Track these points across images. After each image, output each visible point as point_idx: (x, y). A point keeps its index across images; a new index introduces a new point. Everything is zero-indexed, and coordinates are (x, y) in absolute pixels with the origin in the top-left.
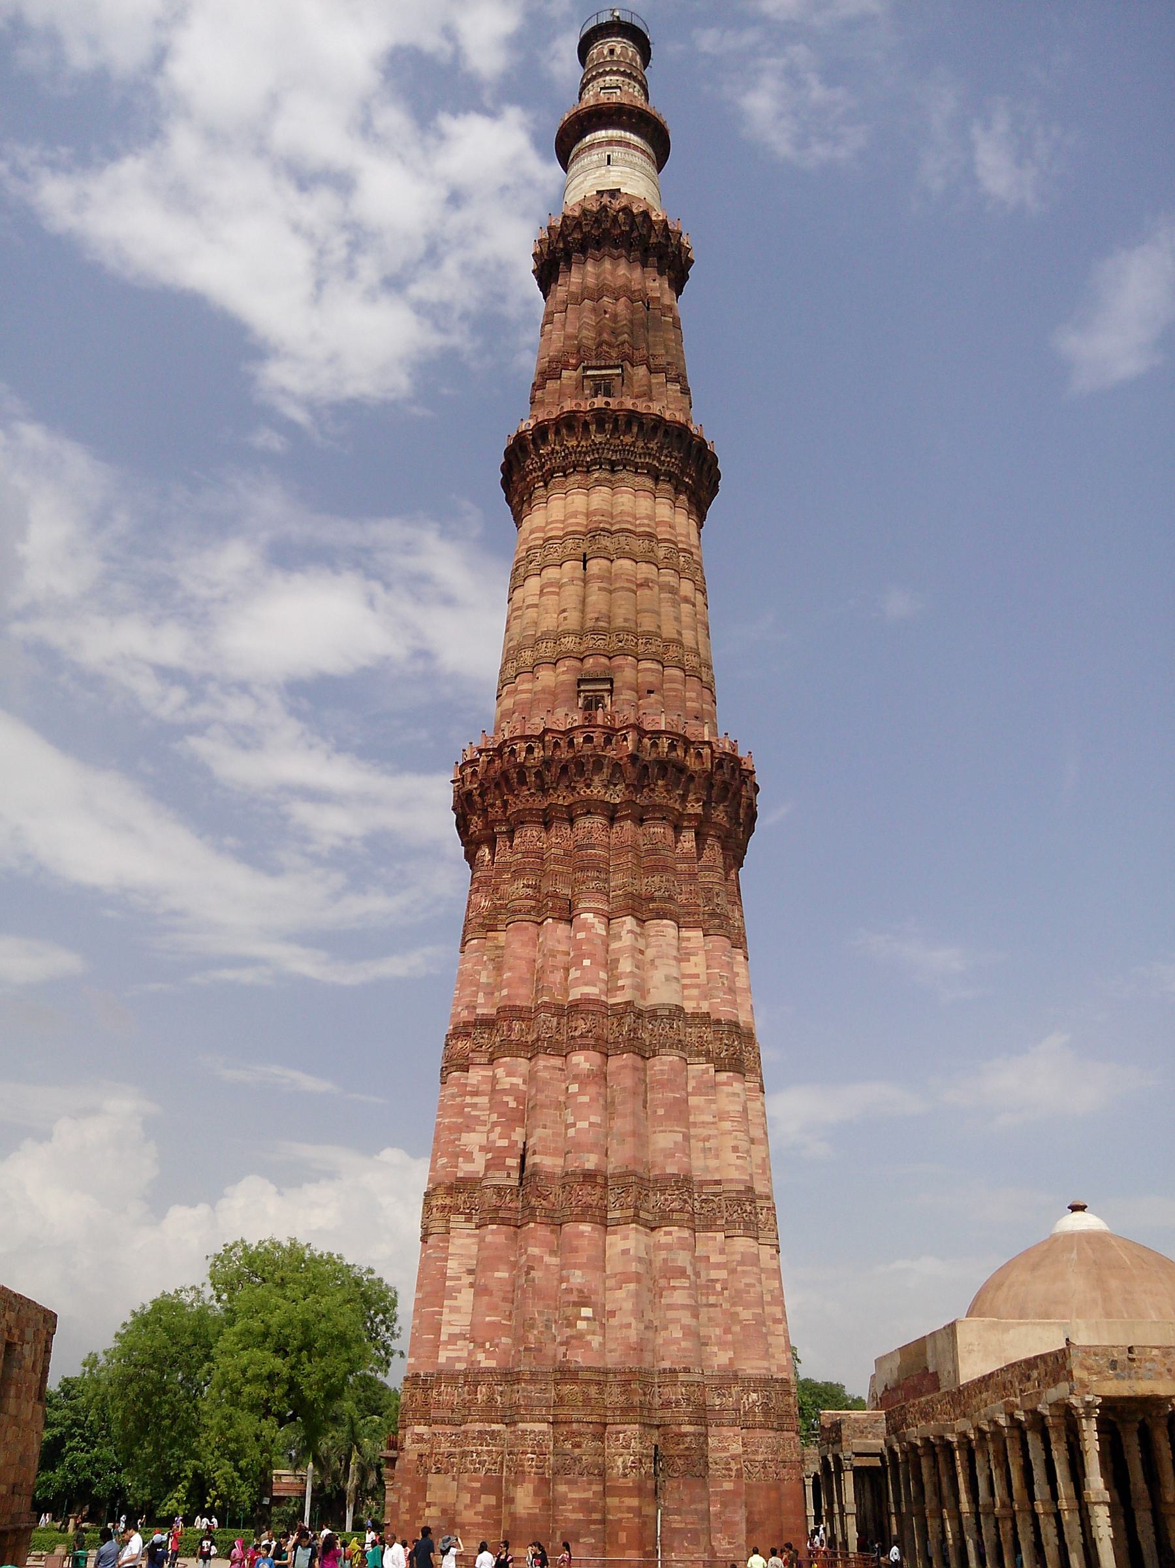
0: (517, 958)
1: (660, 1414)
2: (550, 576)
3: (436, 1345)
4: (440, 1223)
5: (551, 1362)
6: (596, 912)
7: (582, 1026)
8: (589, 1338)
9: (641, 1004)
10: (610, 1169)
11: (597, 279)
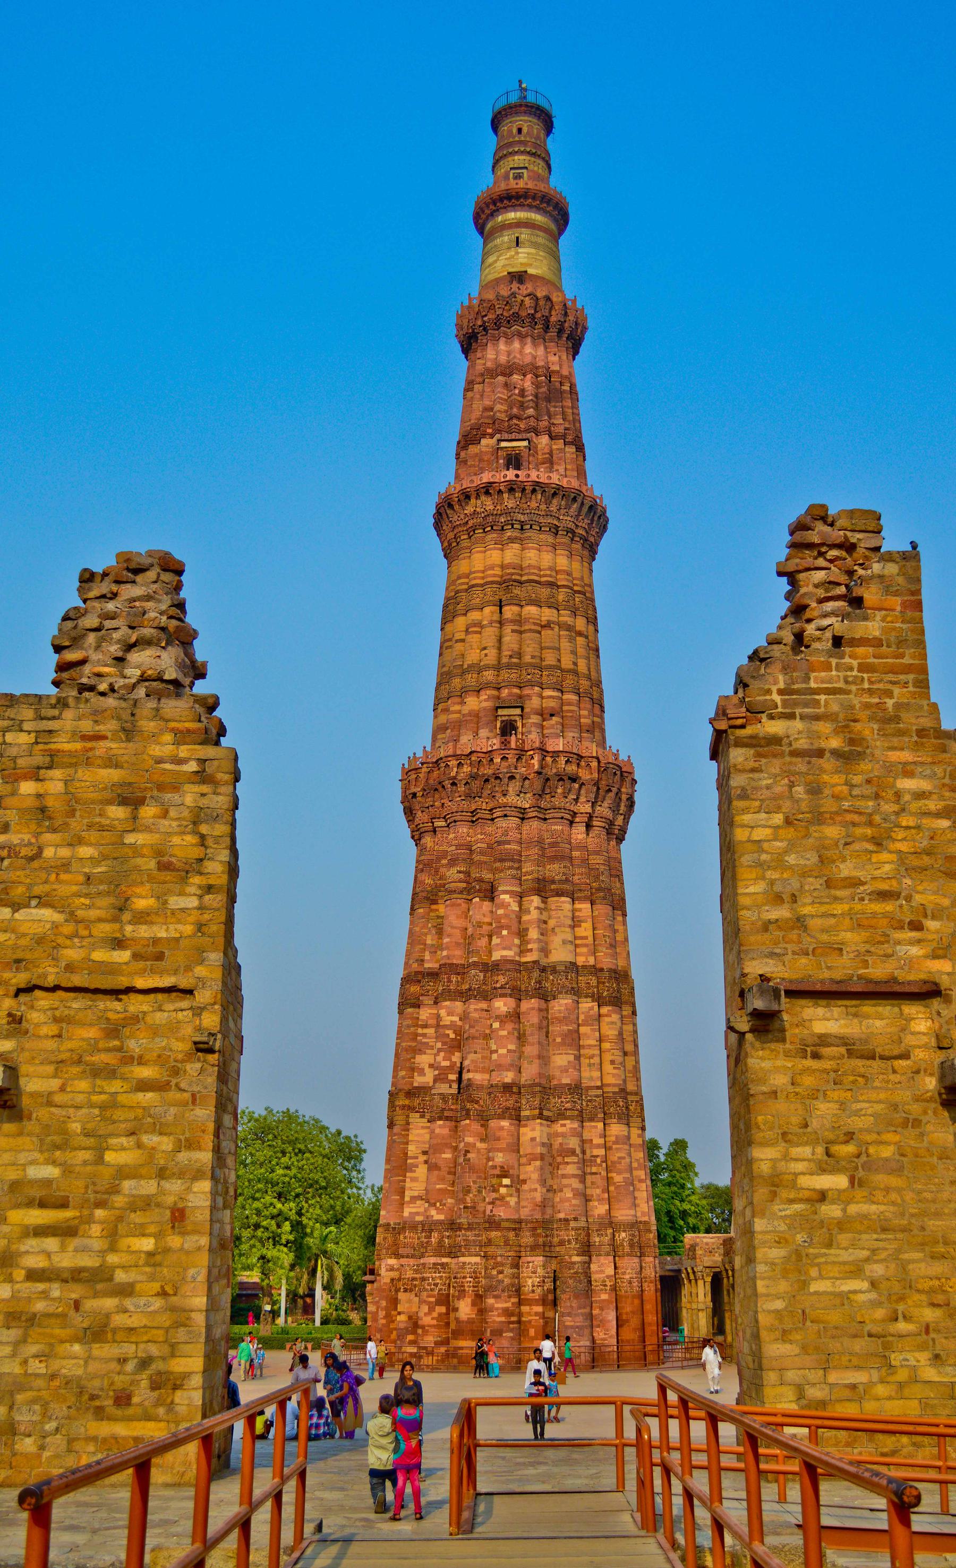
0: (452, 927)
1: (557, 1249)
3: (402, 1204)
7: (502, 980)
8: (508, 1199)
9: (544, 962)
10: (523, 1081)
11: (509, 355)
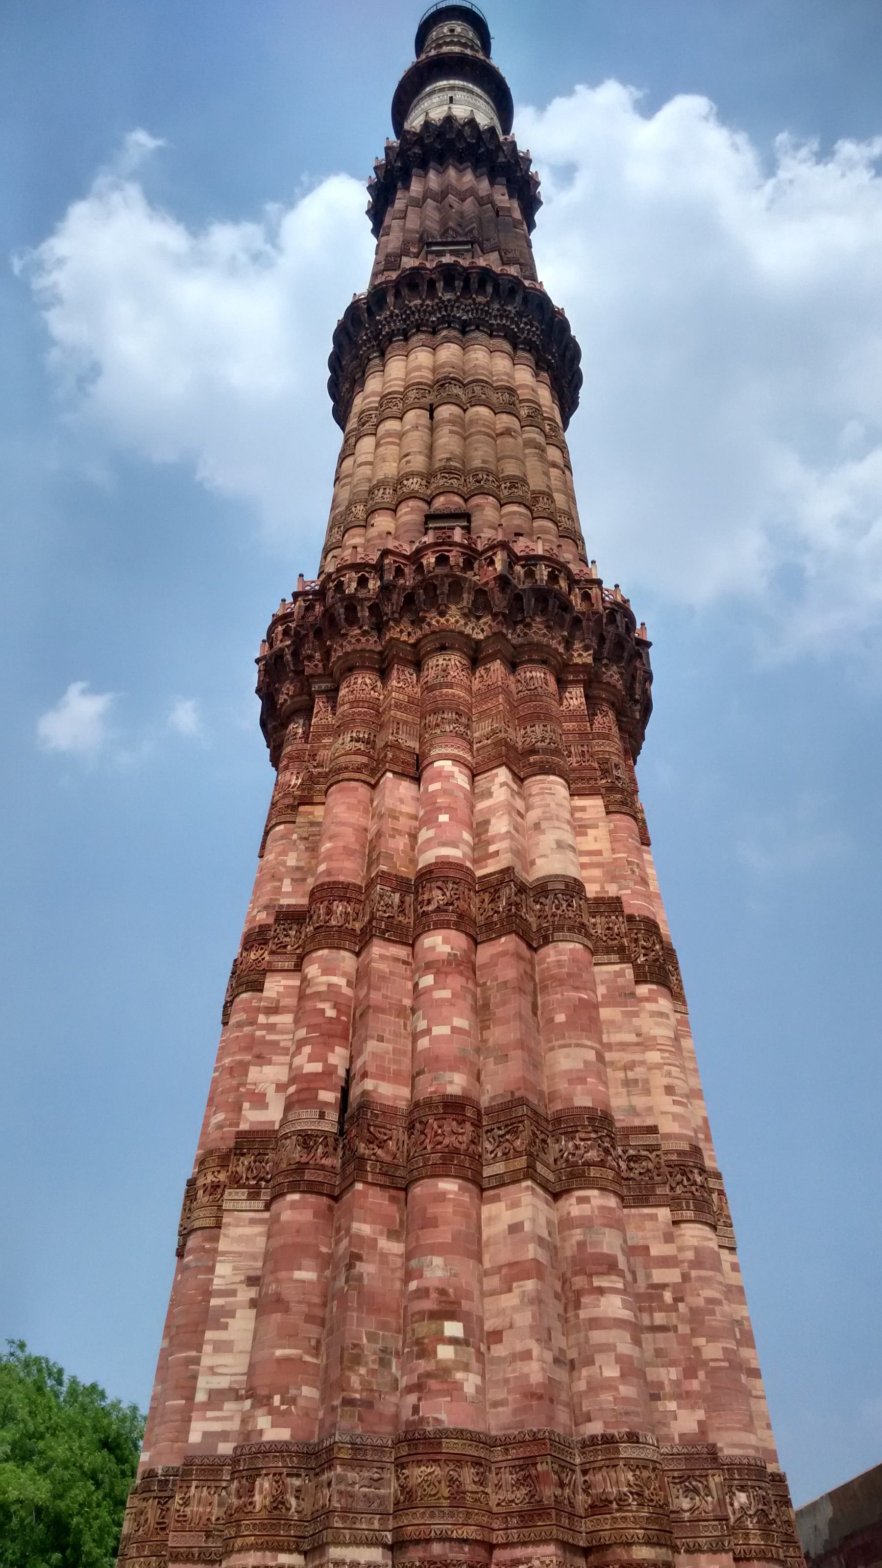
2: (386, 428)
4: (206, 1212)
5: (389, 1429)
6: (456, 760)
8: (459, 1375)
10: (485, 1101)
